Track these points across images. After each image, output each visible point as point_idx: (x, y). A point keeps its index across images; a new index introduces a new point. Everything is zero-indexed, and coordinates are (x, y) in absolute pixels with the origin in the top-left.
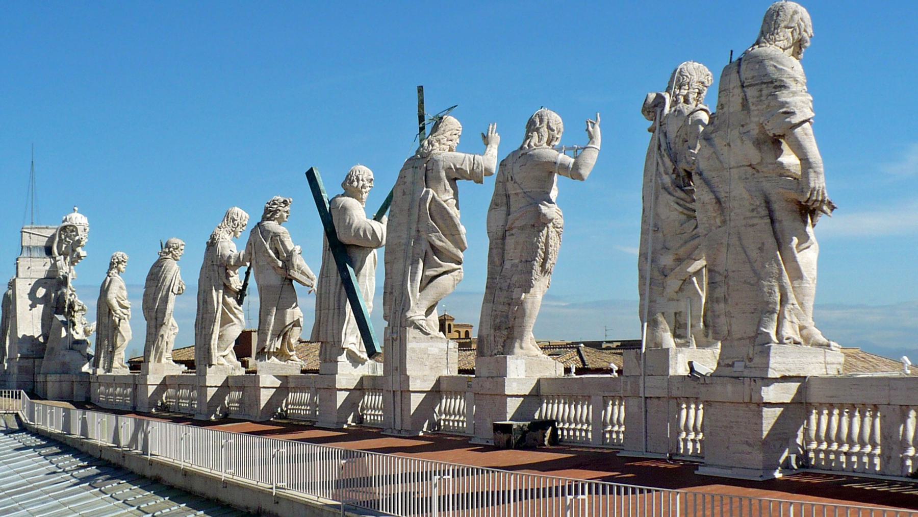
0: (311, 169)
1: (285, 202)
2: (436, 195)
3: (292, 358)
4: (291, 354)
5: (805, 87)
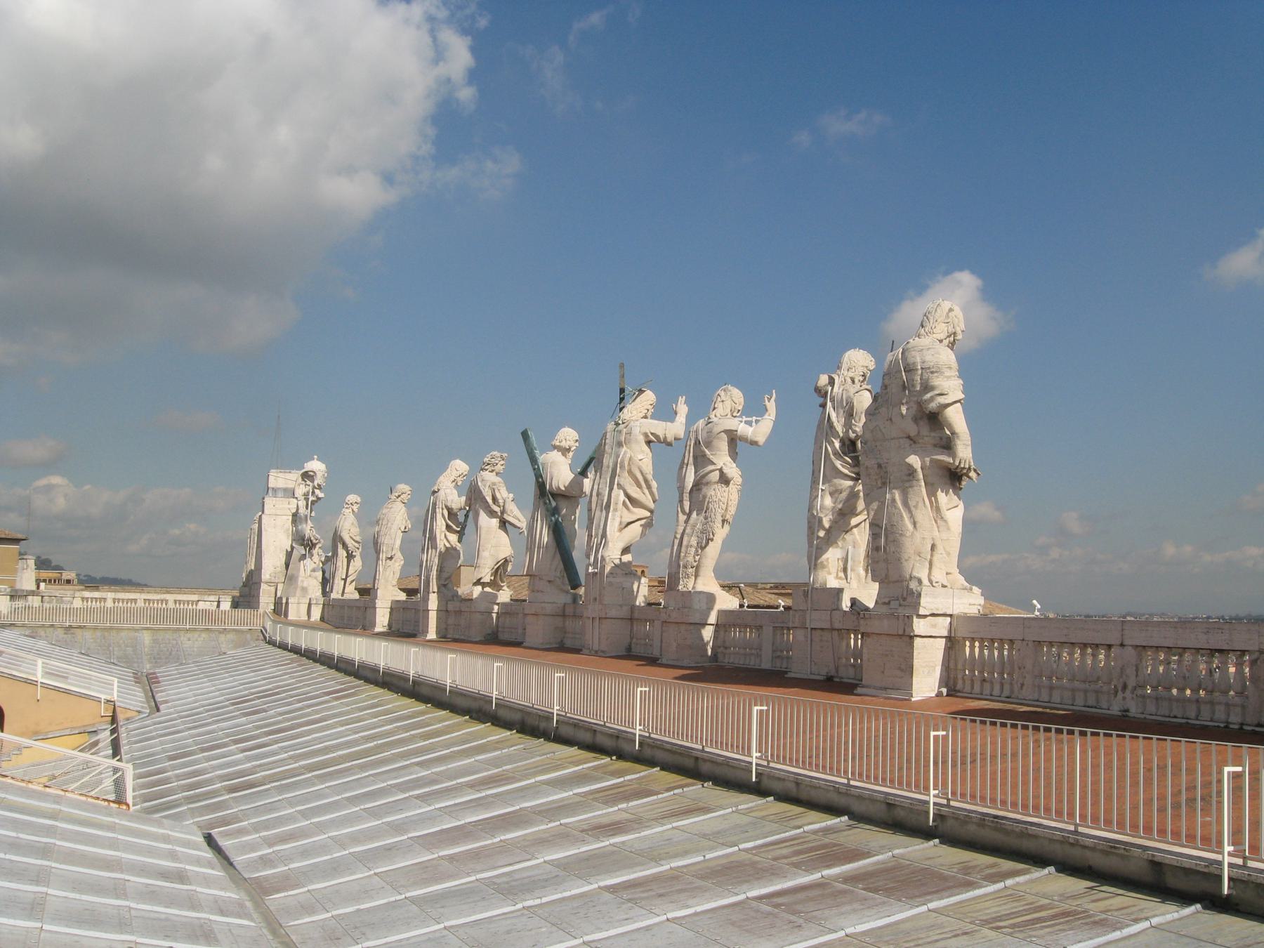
0: (526, 430)
2: (633, 455)
3: (503, 588)
4: (502, 584)
5: (957, 373)
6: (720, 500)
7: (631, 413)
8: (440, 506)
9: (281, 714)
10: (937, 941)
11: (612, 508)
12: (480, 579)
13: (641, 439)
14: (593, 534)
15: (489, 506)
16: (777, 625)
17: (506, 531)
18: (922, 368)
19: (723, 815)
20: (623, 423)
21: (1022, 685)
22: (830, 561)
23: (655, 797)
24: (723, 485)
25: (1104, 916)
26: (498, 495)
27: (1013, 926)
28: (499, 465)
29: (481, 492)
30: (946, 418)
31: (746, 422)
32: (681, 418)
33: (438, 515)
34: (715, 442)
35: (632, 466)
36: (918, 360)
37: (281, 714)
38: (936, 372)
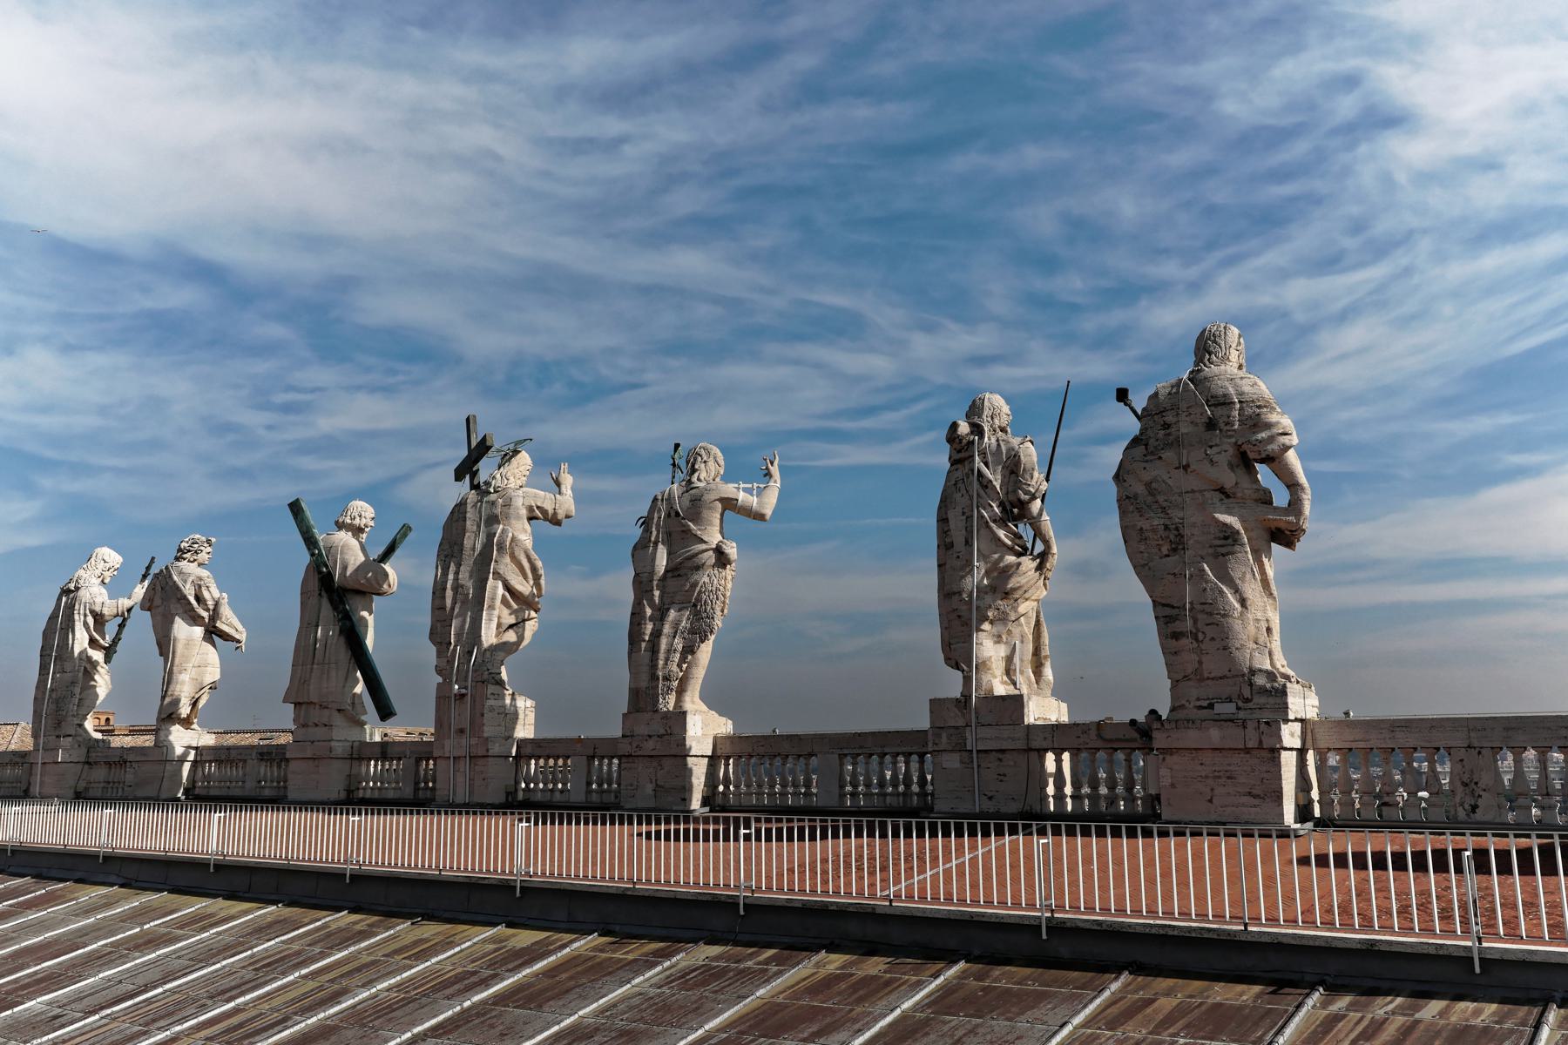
0: (298, 500)
1: (208, 542)
2: (515, 534)
6: (717, 589)
7: (508, 480)
8: (82, 612)
11: (486, 606)
12: (172, 714)
13: (524, 512)
14: (452, 641)
15: (193, 609)
16: (846, 752)
17: (214, 645)
18: (1240, 402)
20: (496, 492)
22: (993, 660)
24: (720, 570)
26: (206, 594)
28: (204, 553)
29: (181, 590)
30: (1287, 464)
31: (745, 490)
33: (77, 623)
34: (705, 513)
35: (516, 549)
36: (1232, 391)
38: (1265, 407)
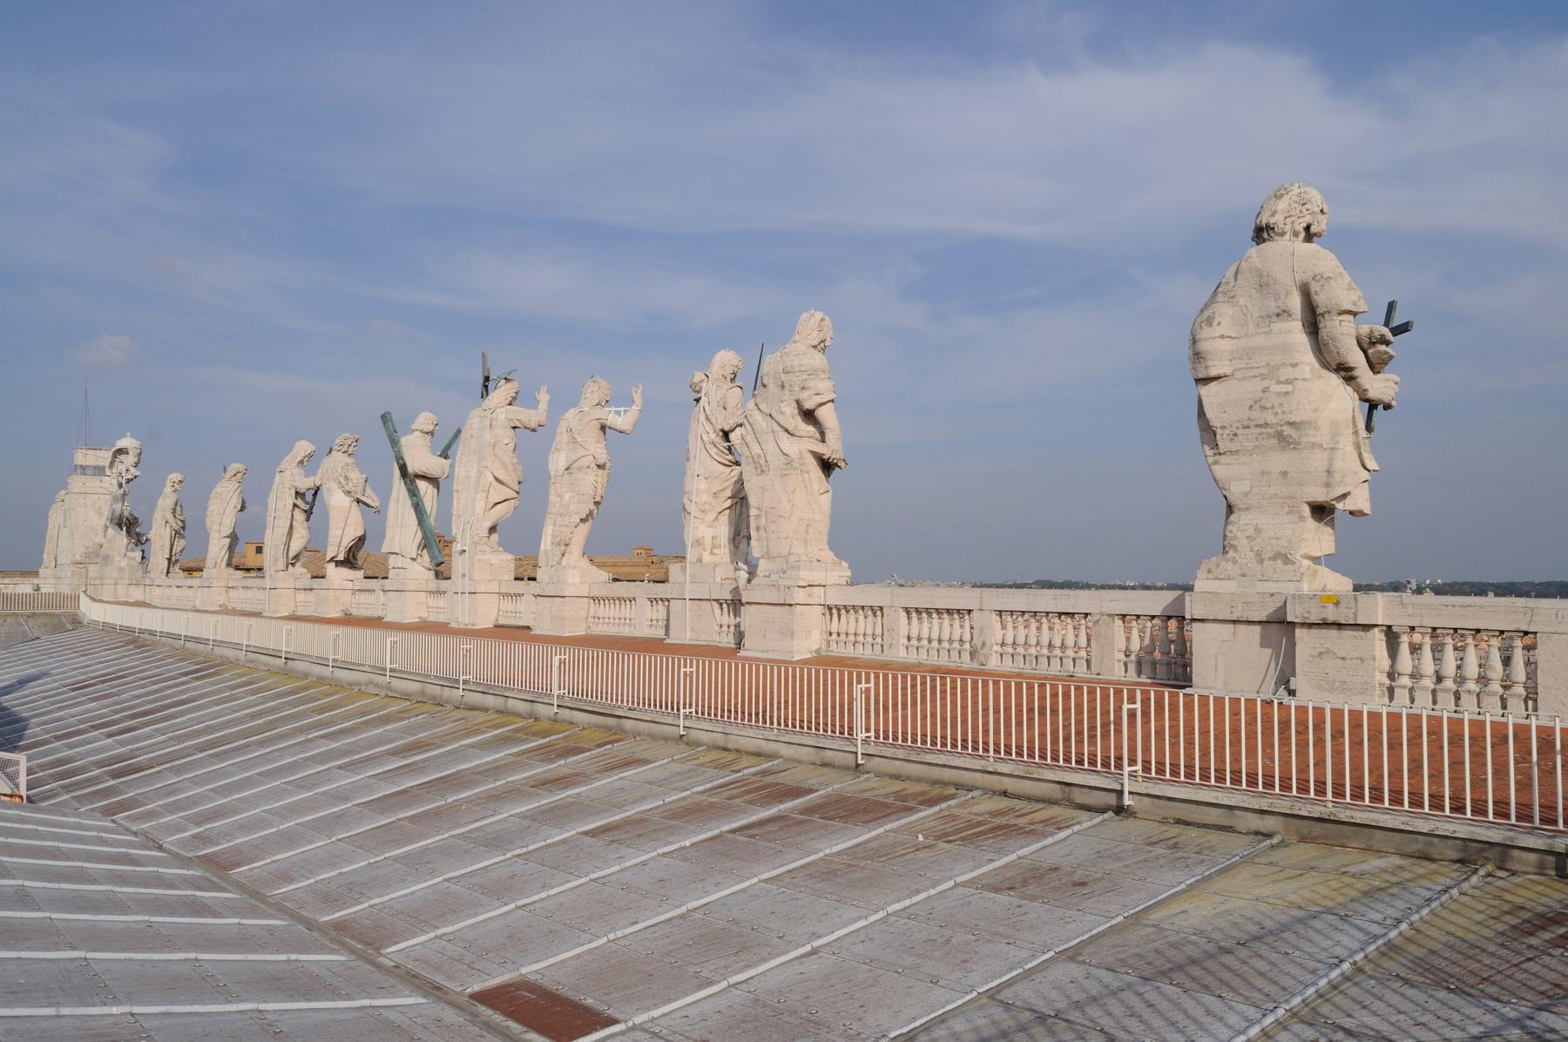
9: (137, 697)
10: (904, 855)
19: (662, 765)
21: (891, 645)
23: (588, 753)
25: (1032, 827)
27: (962, 839)
31: (616, 412)
32: (543, 406)
37: (137, 697)
